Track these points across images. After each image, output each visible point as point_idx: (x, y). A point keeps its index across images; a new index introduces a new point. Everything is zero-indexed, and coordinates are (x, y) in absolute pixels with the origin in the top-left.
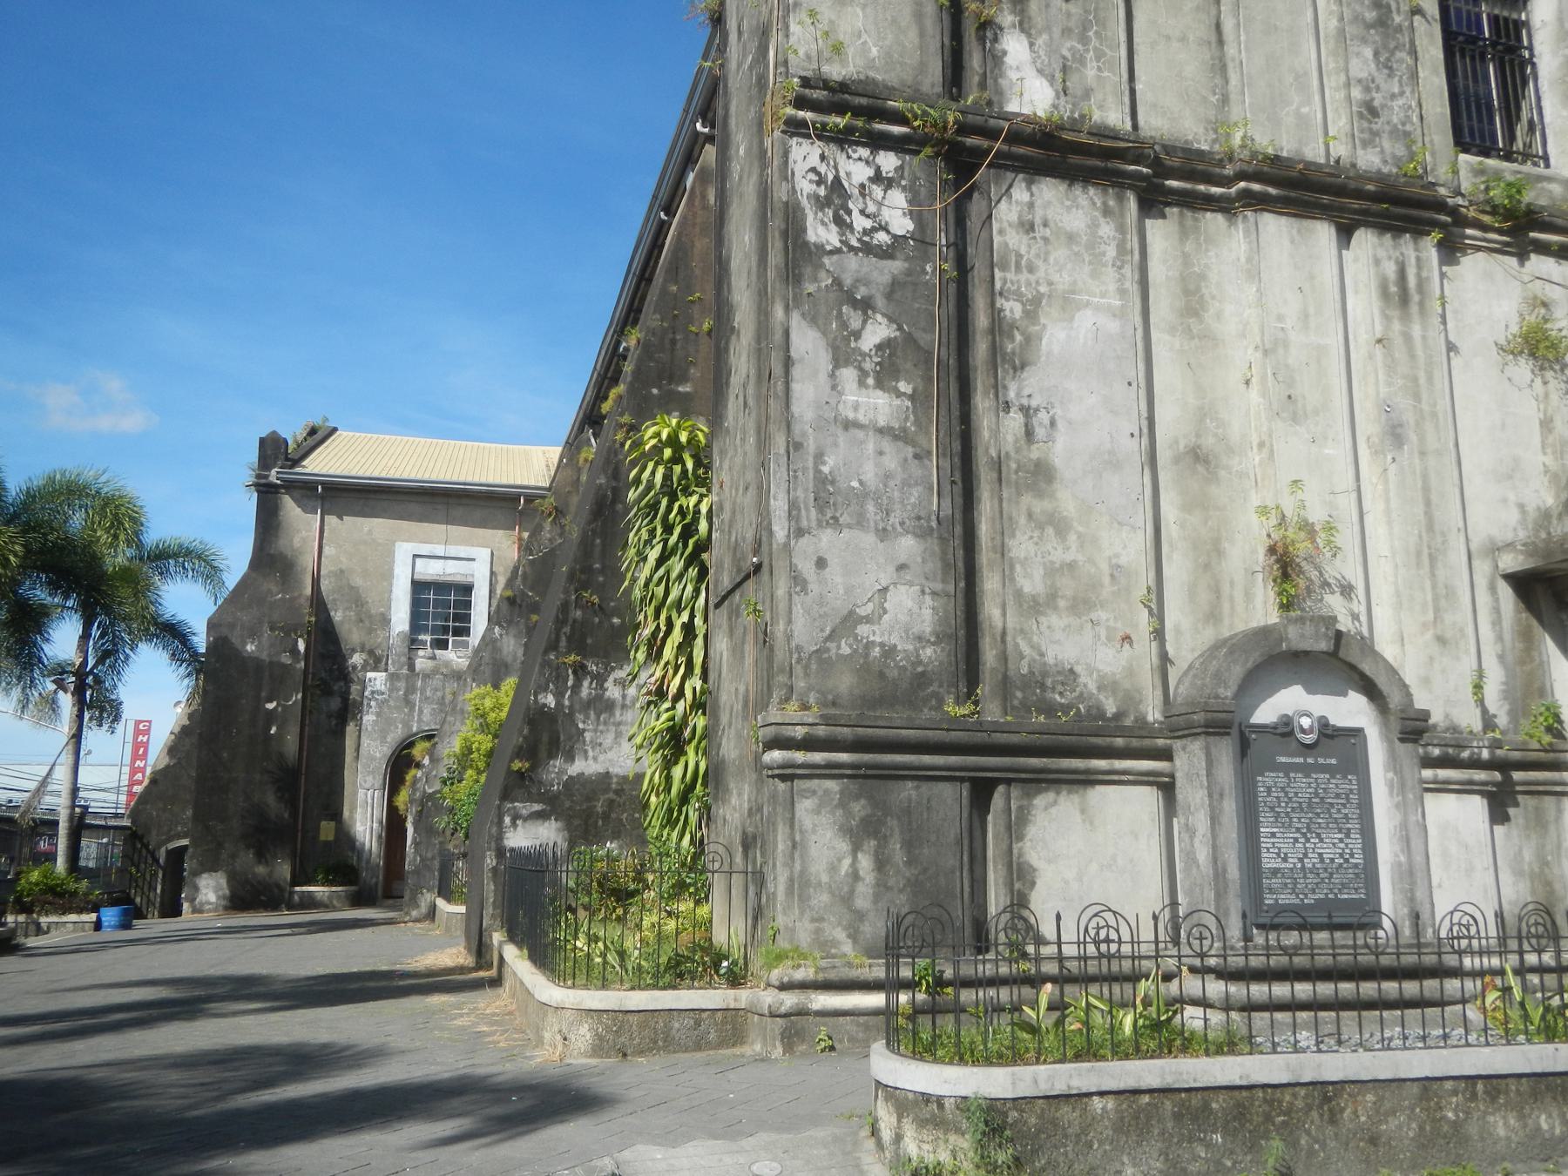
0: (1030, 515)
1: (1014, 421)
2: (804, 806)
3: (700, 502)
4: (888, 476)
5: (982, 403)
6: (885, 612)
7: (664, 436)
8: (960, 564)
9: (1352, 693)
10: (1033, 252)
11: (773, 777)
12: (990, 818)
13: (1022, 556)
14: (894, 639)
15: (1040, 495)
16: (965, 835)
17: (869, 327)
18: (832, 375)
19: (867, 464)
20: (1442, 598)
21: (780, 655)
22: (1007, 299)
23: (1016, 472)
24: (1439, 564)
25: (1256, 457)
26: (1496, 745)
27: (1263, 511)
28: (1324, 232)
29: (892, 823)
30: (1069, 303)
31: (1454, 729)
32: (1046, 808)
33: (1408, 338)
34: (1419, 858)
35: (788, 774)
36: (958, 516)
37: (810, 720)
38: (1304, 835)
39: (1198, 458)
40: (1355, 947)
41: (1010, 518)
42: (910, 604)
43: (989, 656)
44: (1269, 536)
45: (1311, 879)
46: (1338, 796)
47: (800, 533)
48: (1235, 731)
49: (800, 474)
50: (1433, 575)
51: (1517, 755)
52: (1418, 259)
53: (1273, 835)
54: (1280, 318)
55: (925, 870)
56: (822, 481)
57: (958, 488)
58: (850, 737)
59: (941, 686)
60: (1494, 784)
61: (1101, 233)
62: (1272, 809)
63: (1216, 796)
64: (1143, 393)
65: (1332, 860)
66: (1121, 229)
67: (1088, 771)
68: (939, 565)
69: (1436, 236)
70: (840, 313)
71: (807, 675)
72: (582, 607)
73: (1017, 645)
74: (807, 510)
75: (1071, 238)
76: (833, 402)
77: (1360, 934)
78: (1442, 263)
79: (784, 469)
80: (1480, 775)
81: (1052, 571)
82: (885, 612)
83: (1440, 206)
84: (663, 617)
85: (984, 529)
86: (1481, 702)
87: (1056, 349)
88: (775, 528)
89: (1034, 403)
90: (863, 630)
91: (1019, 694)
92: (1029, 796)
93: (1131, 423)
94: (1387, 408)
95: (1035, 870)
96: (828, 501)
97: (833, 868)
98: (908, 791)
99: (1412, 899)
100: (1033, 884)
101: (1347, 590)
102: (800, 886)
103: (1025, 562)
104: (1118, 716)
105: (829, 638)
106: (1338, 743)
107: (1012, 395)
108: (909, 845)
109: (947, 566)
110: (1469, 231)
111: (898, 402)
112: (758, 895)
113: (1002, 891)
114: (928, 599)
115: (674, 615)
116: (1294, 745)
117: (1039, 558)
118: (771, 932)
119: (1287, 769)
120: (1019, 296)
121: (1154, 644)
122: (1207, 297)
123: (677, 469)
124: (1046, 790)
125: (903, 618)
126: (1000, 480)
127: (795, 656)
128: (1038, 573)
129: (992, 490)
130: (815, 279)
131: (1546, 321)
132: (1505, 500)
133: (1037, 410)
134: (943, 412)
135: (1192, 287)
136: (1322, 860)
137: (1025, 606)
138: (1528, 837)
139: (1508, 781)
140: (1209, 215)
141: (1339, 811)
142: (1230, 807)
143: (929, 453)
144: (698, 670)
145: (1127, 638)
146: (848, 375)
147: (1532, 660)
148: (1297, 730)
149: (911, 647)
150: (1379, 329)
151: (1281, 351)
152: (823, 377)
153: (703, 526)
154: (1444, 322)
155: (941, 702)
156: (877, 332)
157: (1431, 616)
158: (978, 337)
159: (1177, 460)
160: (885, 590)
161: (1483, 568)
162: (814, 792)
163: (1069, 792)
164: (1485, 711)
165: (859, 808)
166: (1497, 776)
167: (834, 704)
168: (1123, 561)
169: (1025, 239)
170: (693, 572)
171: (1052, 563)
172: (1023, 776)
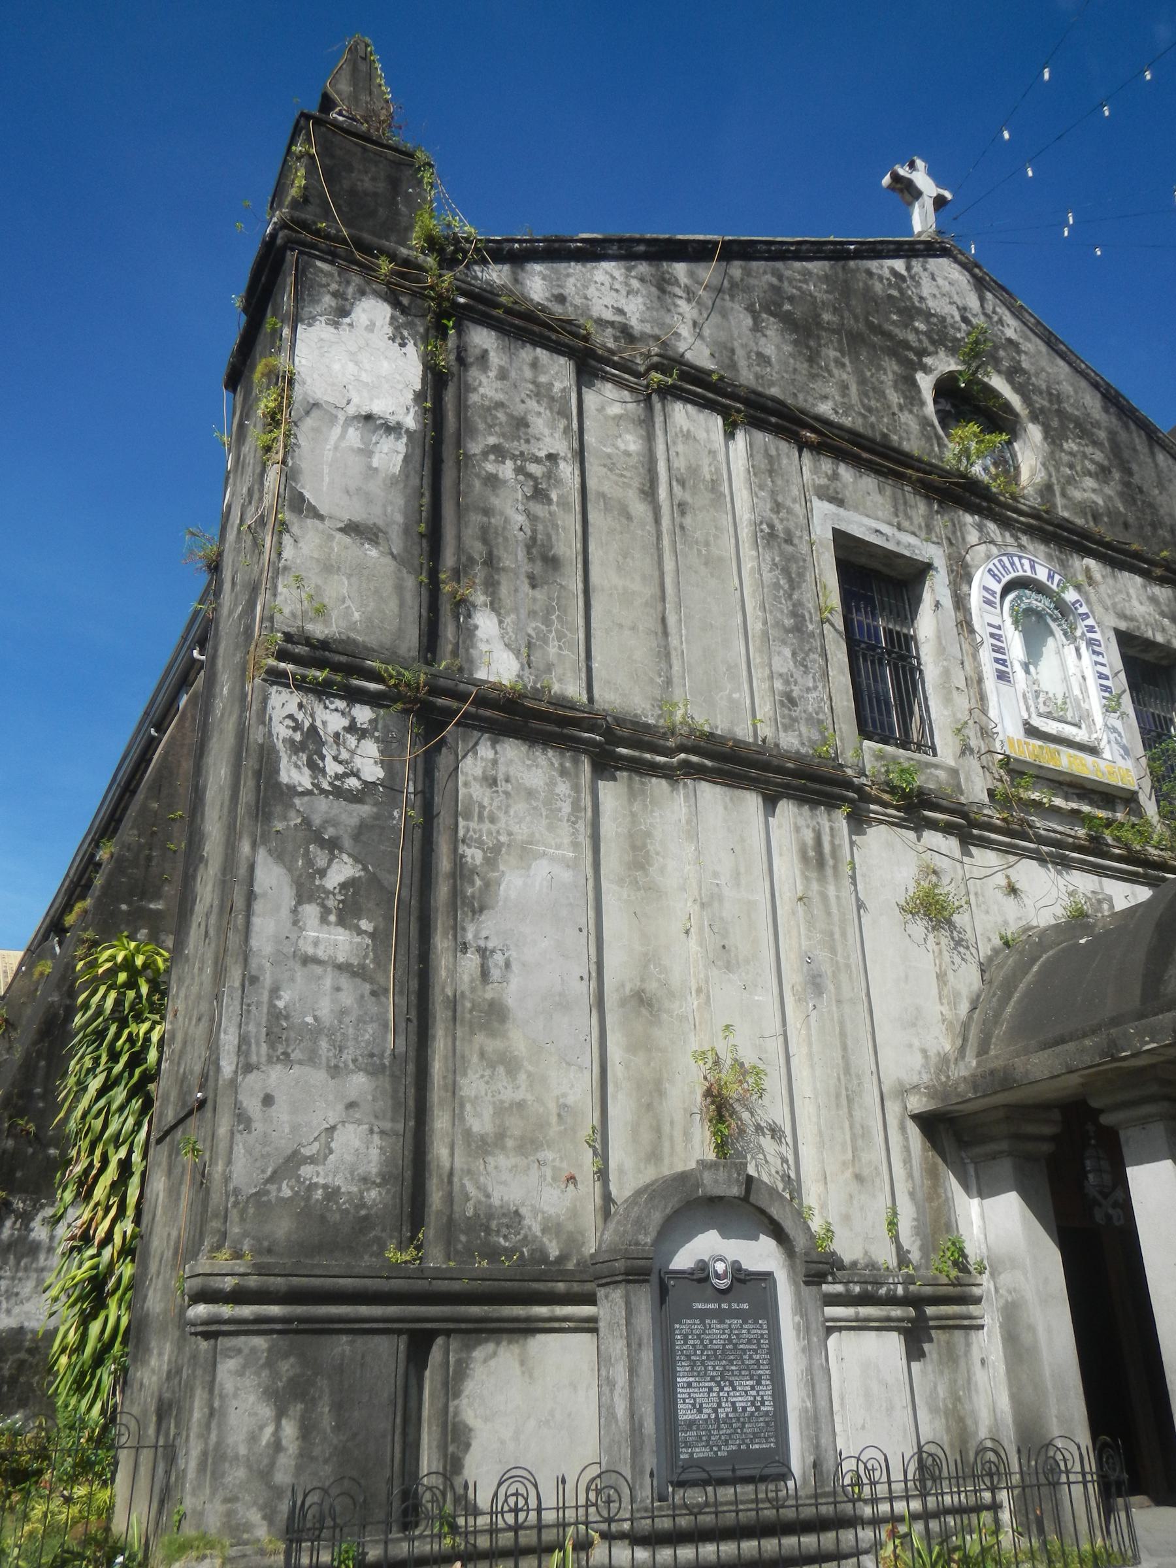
0: (482, 1054)
1: (470, 962)
2: (227, 1367)
3: (152, 1029)
4: (343, 1012)
5: (441, 943)
6: (331, 1152)
7: (120, 959)
8: (411, 1103)
9: (762, 1237)
10: (495, 804)
11: (196, 1334)
12: (427, 1373)
13: (473, 1094)
14: (338, 1181)
15: (492, 1034)
16: (400, 1393)
17: (335, 866)
18: (295, 911)
19: (321, 999)
20: (859, 1136)
21: (216, 1198)
22: (469, 846)
23: (471, 1011)
24: (856, 1106)
25: (694, 1002)
26: (909, 1280)
27: (701, 1056)
28: (752, 802)
29: (323, 1383)
30: (526, 852)
31: (872, 1266)
32: (485, 1361)
33: (824, 897)
34: (823, 1403)
35: (212, 1331)
36: (412, 1054)
37: (242, 1270)
38: (718, 1384)
39: (642, 1001)
40: (757, 1501)
41: (463, 1057)
42: (357, 1143)
43: (435, 1198)
44: (705, 1078)
46: (749, 1341)
47: (248, 1068)
48: (654, 1278)
49: (253, 1008)
50: (851, 1115)
51: (928, 1290)
52: (832, 829)
53: (689, 1385)
54: (716, 875)
55: (355, 1435)
56: (276, 1016)
57: (413, 1027)
58: (284, 1289)
59: (384, 1230)
60: (909, 1320)
61: (557, 791)
62: (688, 1357)
63: (634, 1347)
64: (592, 938)
65: (744, 1409)
66: (576, 788)
67: (528, 1319)
68: (390, 1102)
69: (846, 809)
70: (307, 851)
71: (242, 1219)
72: (15, 1137)
73: (463, 1186)
74: (258, 1044)
75: (530, 794)
76: (293, 936)
77: (762, 1487)
78: (851, 833)
79: (237, 1003)
80: (896, 1312)
81: (501, 1110)
82: (331, 1152)
83: (848, 784)
84: (98, 1152)
85: (437, 1067)
86: (896, 1238)
87: (513, 895)
88: (223, 1063)
89: (490, 945)
90: (306, 1171)
91: (463, 1238)
92: (469, 1348)
93: (580, 967)
94: (809, 960)
95: (470, 1430)
96: (280, 1036)
97: (253, 1438)
98: (342, 1346)
99: (817, 1447)
100: (468, 1446)
101: (775, 1132)
102: (214, 1461)
103: (475, 1101)
104: (562, 1259)
105: (270, 1180)
106: (750, 1286)
107: (470, 936)
108: (338, 1407)
109: (397, 1105)
110: (872, 807)
111: (358, 939)
112: (168, 1473)
113: (435, 1456)
114: (376, 1139)
115: (111, 1150)
116: (710, 1291)
117: (489, 1097)
118: (176, 1518)
119: (703, 1315)
120: (480, 844)
121: (598, 1184)
122: (652, 853)
123: (131, 994)
124: (487, 1341)
125: (349, 1158)
126: (454, 1019)
127: (232, 1199)
128: (488, 1112)
129: (447, 1028)
130: (285, 818)
131: (936, 886)
132: (910, 1046)
133: (493, 951)
134: (402, 951)
135: (639, 843)
136: (735, 1410)
137: (473, 1146)
138: (942, 1373)
139: (921, 1315)
140: (654, 780)
141: (751, 1357)
142: (647, 1357)
143: (386, 990)
144: (130, 1212)
145: (572, 1179)
146: (311, 911)
147: (939, 1196)
148: (712, 1275)
149: (355, 1189)
150: (800, 887)
151: (716, 904)
152: (285, 913)
153: (152, 1055)
154: (855, 884)
155: (383, 1247)
156: (342, 871)
157: (849, 1155)
158: (441, 879)
159: (623, 1002)
160: (332, 1129)
161: (894, 1109)
162: (239, 1351)
163: (510, 1342)
164: (899, 1247)
165: (286, 1367)
166: (911, 1312)
167: (269, 1251)
168: (570, 1100)
169: (488, 792)
170: (136, 1104)
171: (502, 1102)
172: (463, 1326)
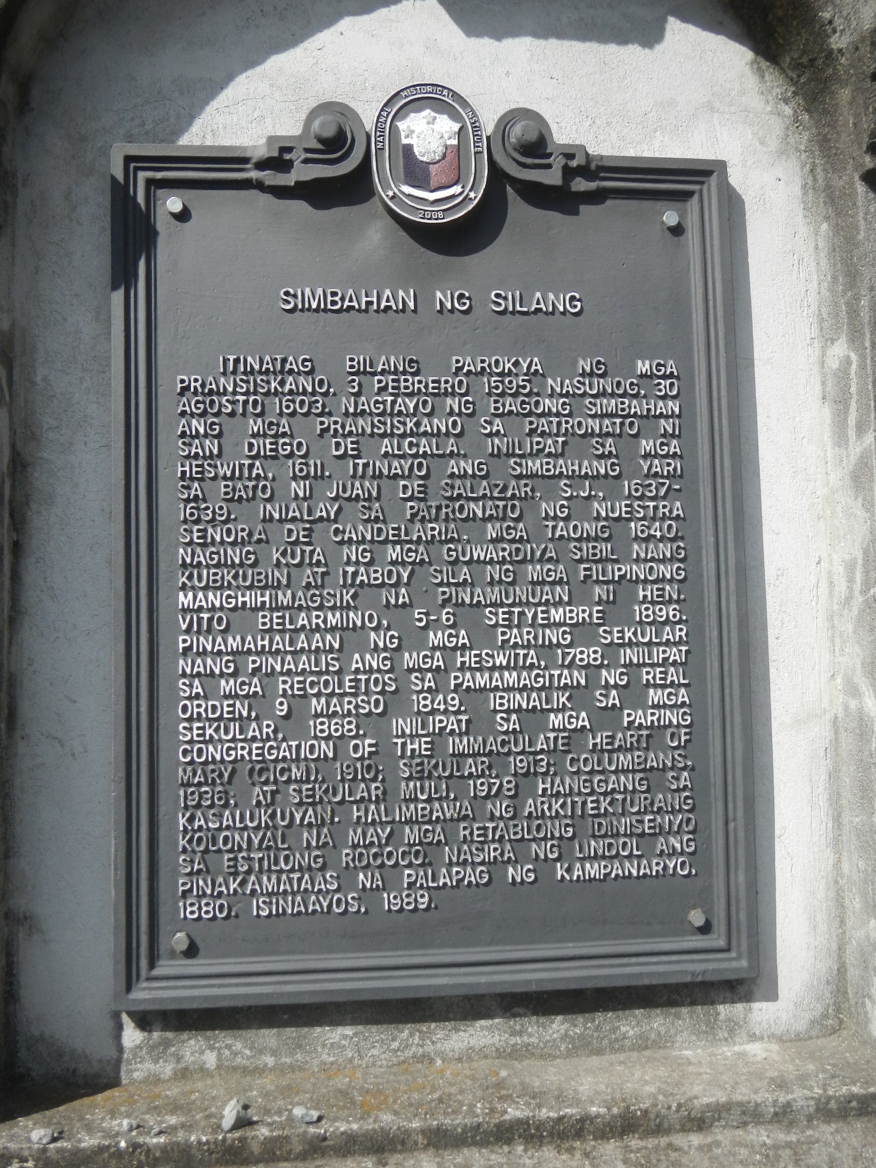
9: (674, 25)
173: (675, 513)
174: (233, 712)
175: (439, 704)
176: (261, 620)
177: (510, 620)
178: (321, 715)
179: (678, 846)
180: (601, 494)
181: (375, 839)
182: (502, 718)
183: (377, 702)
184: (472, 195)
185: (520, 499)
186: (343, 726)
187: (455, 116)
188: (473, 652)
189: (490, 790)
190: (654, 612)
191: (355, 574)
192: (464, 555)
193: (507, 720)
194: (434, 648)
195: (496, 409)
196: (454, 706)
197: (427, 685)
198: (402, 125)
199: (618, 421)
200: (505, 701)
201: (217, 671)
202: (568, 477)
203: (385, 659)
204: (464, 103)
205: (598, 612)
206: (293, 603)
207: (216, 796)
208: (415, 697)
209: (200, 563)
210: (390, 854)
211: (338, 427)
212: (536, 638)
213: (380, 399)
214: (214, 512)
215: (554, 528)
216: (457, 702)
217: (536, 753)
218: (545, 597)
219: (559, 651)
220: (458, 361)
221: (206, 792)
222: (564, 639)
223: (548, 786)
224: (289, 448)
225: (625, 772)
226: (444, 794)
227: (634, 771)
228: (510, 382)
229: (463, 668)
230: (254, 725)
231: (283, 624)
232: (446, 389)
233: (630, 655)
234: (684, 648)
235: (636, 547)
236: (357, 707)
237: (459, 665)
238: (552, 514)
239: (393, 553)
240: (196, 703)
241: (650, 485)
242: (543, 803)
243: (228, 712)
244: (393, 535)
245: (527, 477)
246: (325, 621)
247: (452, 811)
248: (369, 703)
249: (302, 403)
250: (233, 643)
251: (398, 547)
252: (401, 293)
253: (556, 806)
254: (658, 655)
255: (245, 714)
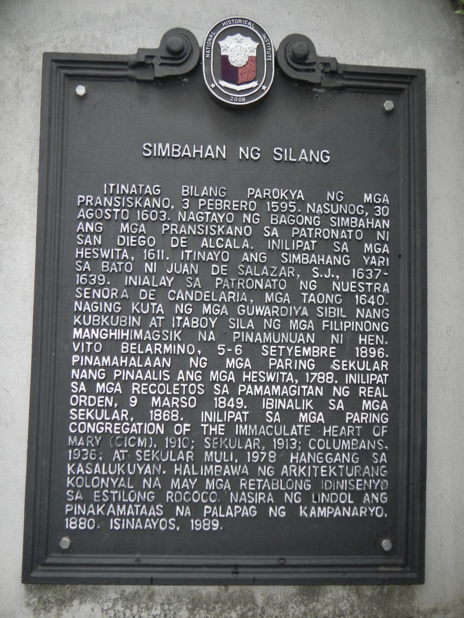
38: (208, 348)
45: (216, 466)
46: (325, 246)
53: (111, 347)
62: (115, 278)
65: (290, 417)
148: (209, 70)
173: (384, 290)
174: (103, 403)
175: (231, 404)
176: (123, 347)
177: (278, 353)
178: (157, 407)
179: (377, 499)
180: (338, 277)
181: (188, 486)
182: (269, 414)
183: (192, 401)
184: (264, 88)
185: (286, 278)
186: (170, 415)
187: (255, 38)
188: (253, 372)
189: (260, 458)
190: (368, 352)
191: (182, 321)
192: (250, 312)
193: (273, 416)
194: (229, 370)
195: (274, 221)
196: (240, 405)
197: (224, 391)
198: (222, 43)
199: (350, 231)
200: (272, 404)
201: (95, 378)
202: (317, 265)
203: (198, 374)
204: (262, 31)
205: (332, 350)
206: (143, 338)
207: (91, 454)
208: (216, 399)
209: (87, 310)
210: (196, 496)
211: (175, 230)
212: (293, 365)
213: (202, 213)
214: (97, 279)
215: (308, 297)
216: (242, 403)
217: (290, 437)
218: (300, 340)
219: (307, 374)
220: (251, 191)
221: (85, 452)
222: (311, 367)
223: (297, 458)
224: (144, 242)
225: (346, 451)
226: (232, 459)
227: (351, 451)
228: (284, 205)
229: (247, 382)
230: (116, 412)
231: (136, 350)
232: (243, 208)
233: (351, 378)
234: (386, 375)
235: (358, 310)
236: (180, 403)
237: (244, 380)
238: (306, 288)
239: (206, 309)
240: (81, 396)
241: (370, 272)
242: (293, 468)
243: (100, 403)
244: (207, 298)
245: (291, 264)
246: (162, 349)
247: (236, 471)
248: (187, 401)
249: (154, 213)
250: (106, 360)
251: (209, 305)
252: (218, 148)
253: (301, 470)
254: (370, 379)
255: (111, 404)
